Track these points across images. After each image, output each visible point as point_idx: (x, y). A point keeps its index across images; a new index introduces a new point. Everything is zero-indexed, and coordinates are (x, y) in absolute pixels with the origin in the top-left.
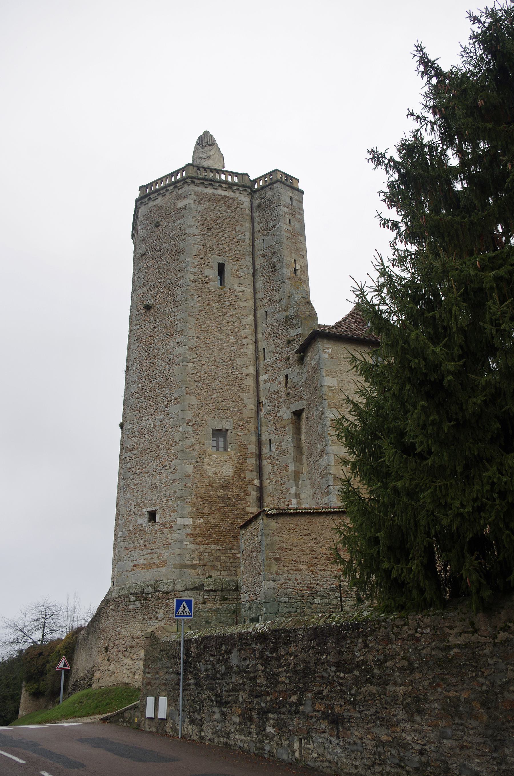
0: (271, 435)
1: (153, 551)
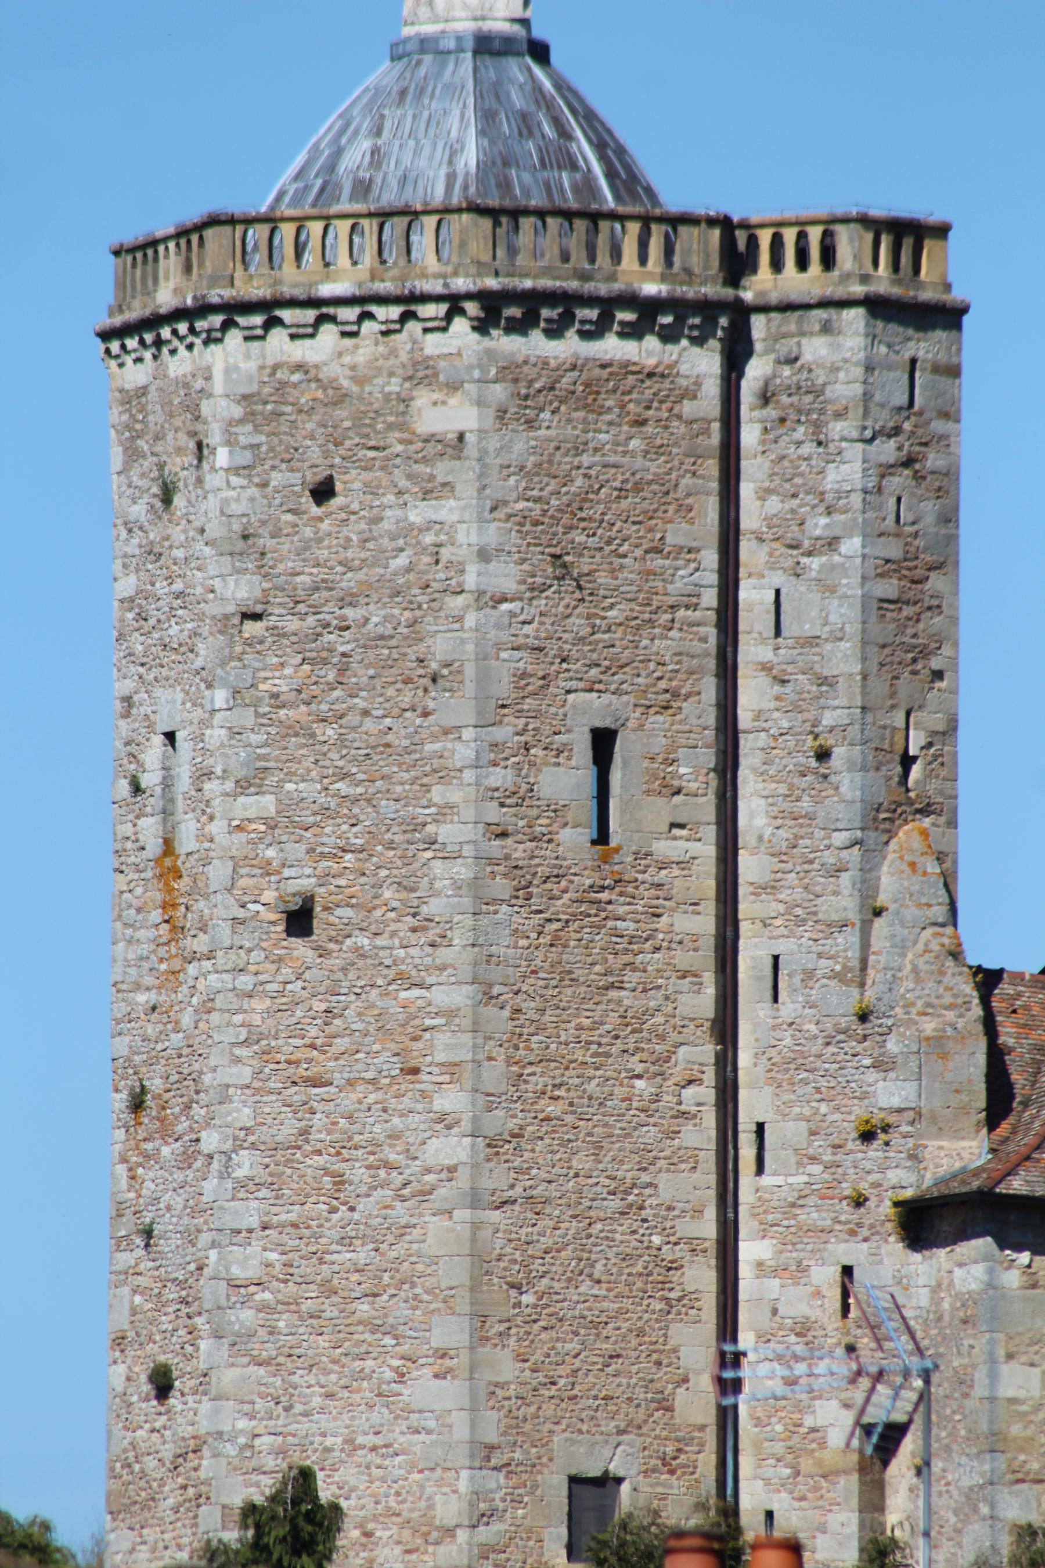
0: (775, 1497)
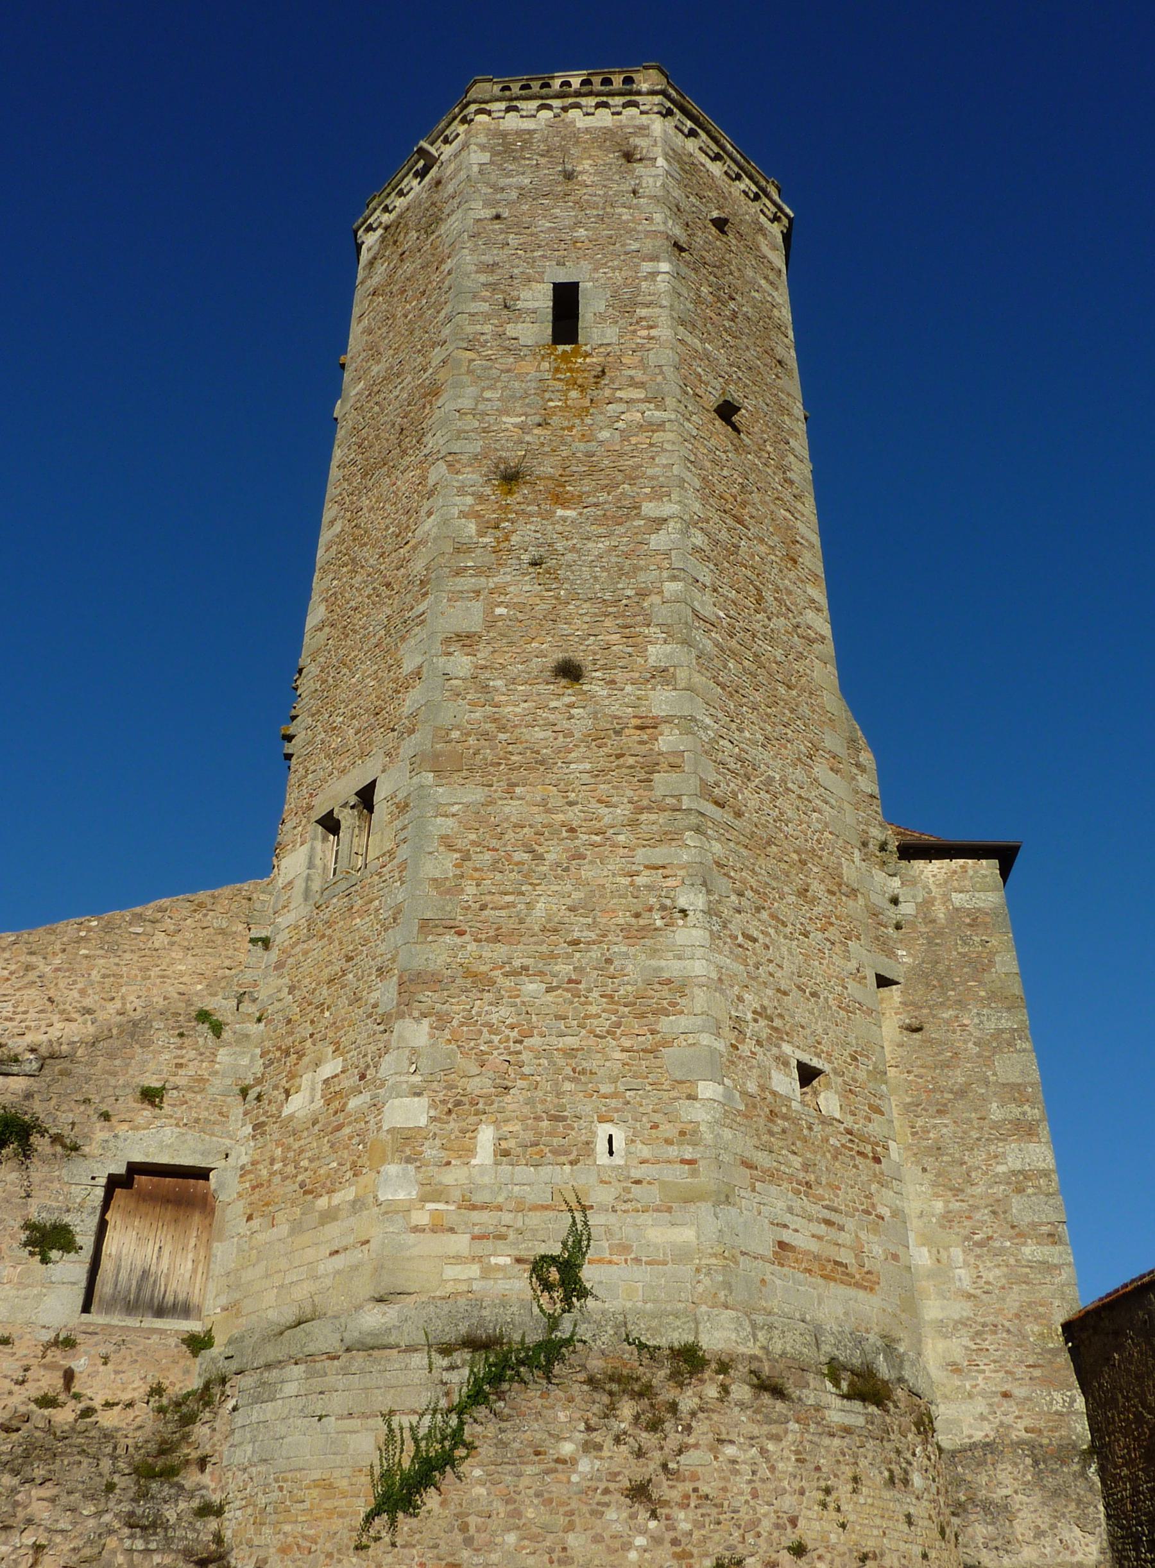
1: (833, 1216)
